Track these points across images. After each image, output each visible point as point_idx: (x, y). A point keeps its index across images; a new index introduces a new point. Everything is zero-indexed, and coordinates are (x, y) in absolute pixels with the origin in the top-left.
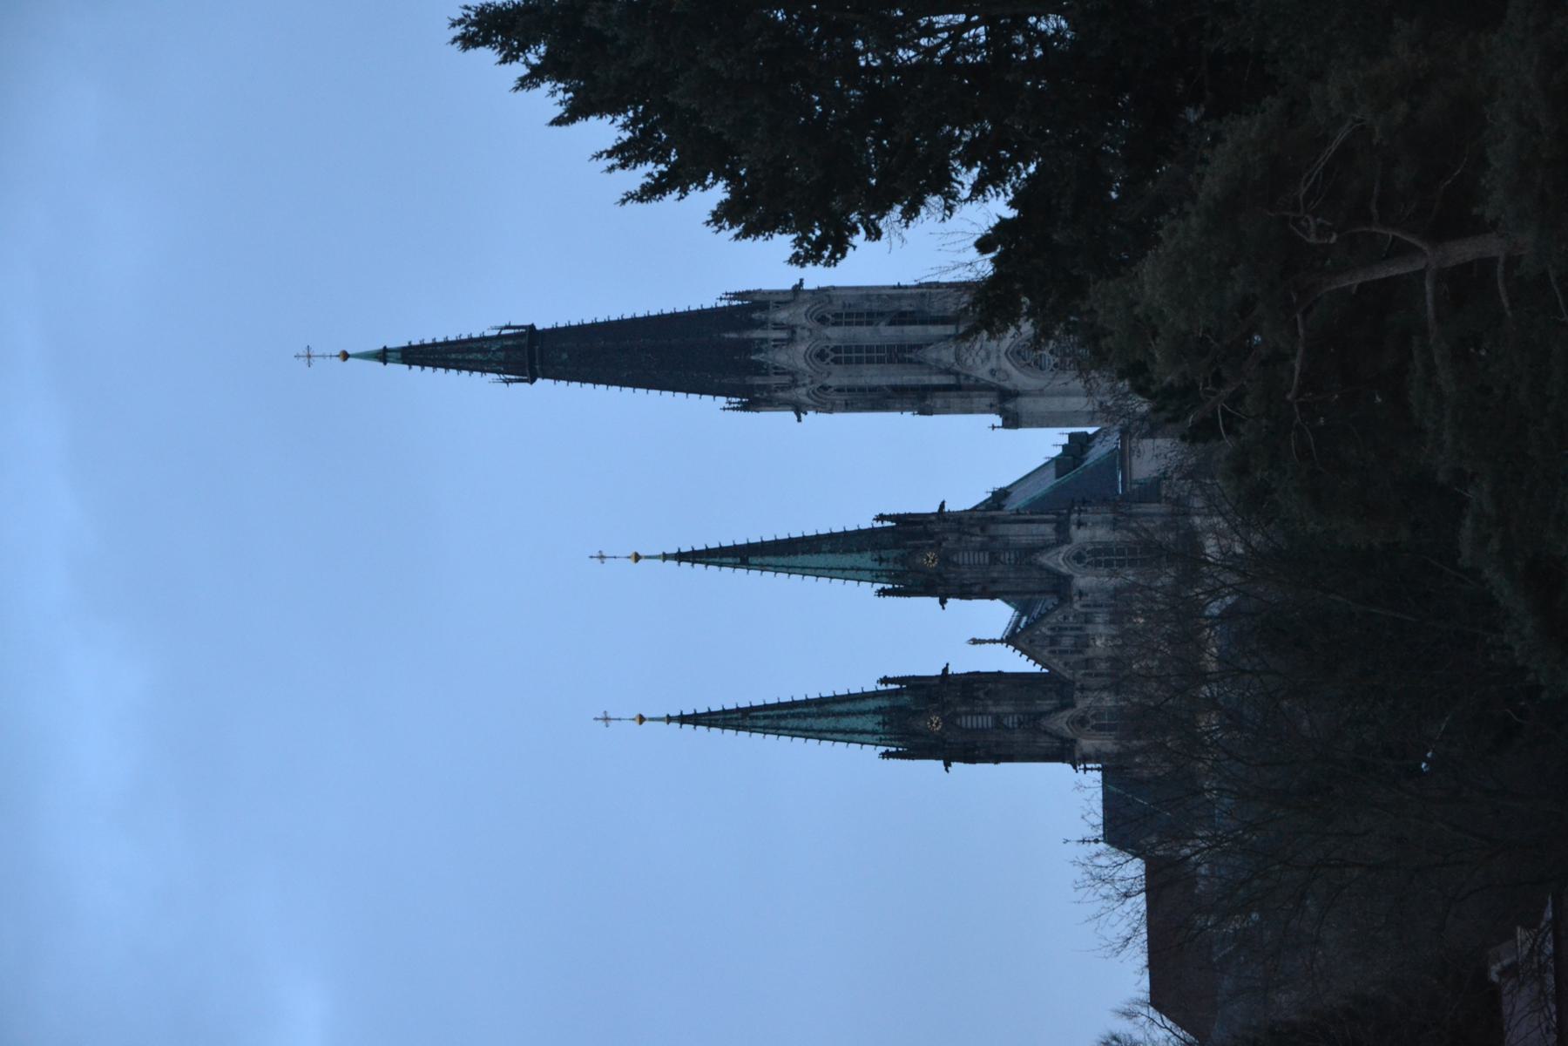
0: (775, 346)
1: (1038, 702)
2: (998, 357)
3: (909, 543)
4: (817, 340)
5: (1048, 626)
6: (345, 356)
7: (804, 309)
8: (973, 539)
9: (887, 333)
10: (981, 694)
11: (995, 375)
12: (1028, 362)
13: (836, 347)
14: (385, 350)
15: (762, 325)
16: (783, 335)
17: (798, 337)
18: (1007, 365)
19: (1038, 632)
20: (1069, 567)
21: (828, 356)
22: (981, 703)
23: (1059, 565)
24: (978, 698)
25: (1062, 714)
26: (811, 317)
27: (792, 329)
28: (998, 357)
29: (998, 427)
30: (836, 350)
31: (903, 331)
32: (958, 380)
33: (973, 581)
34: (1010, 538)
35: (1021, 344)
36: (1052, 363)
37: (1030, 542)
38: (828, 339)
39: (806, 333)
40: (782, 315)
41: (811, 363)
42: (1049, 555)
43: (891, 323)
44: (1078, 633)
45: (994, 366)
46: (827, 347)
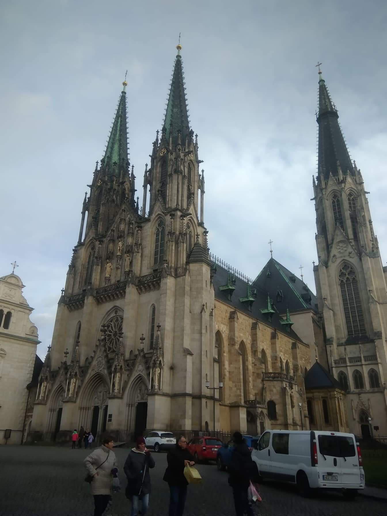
0: (336, 179)
2: (341, 257)
3: (171, 139)
8: (171, 167)
9: (347, 214)
11: (334, 257)
12: (342, 270)
13: (339, 200)
15: (345, 173)
18: (339, 261)
19: (128, 213)
20: (154, 219)
21: (335, 199)
23: (155, 213)
24: (106, 196)
26: (350, 190)
27: (344, 181)
28: (341, 257)
29: (314, 265)
30: (338, 201)
31: (347, 219)
32: (330, 245)
35: (349, 266)
36: (342, 279)
37: (168, 195)
38: (341, 195)
41: (331, 193)
43: (350, 215)
44: (126, 232)
45: (337, 256)
46: (339, 197)
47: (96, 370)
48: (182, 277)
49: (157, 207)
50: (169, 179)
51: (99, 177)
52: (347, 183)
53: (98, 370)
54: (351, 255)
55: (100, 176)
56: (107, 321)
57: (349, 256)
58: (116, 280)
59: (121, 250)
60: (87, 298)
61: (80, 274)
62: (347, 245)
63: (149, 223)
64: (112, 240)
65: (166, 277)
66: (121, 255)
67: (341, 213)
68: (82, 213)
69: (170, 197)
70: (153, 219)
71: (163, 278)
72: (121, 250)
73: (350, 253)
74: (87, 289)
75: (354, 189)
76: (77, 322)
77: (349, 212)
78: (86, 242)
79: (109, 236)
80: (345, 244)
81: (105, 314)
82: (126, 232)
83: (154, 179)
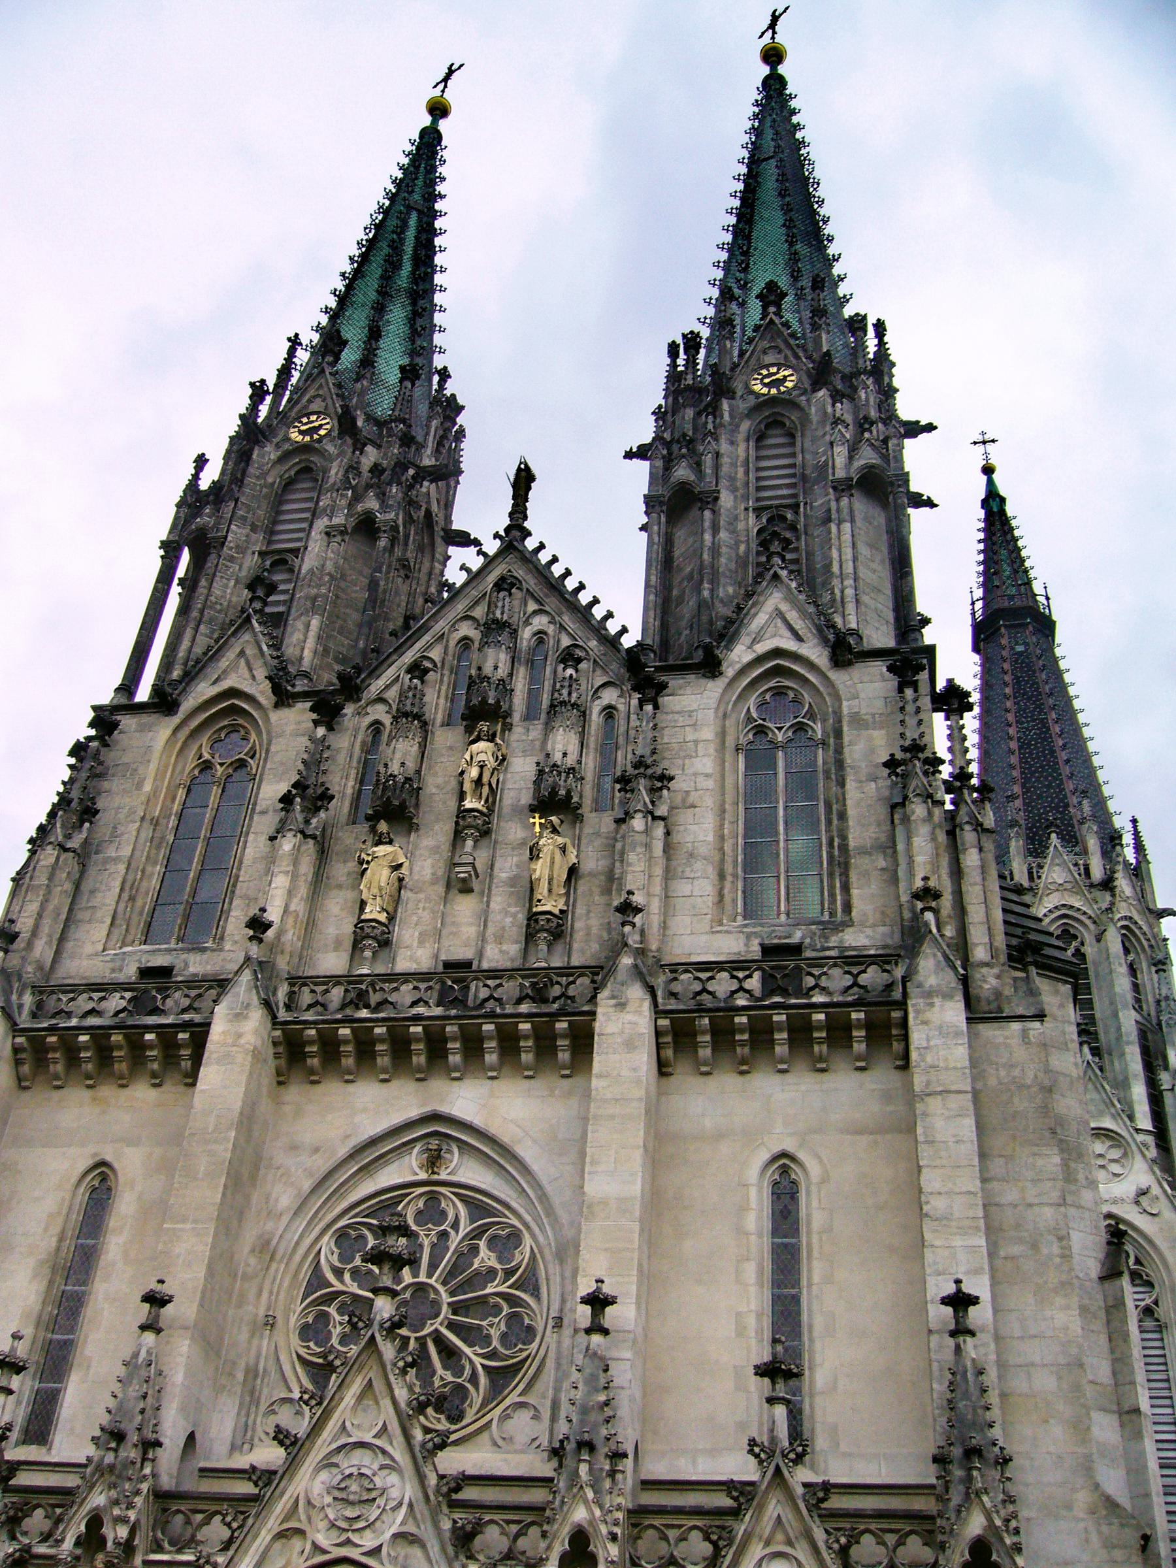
0: (1076, 865)
1: (315, 622)
4: (1095, 922)
5: (551, 629)
6: (988, 470)
7: (1137, 917)
10: (371, 503)
13: (1084, 955)
14: (1003, 500)
16: (1097, 873)
17: (1098, 894)
20: (743, 671)
22: (344, 502)
23: (755, 641)
25: (261, 673)
27: (1107, 884)
31: (1128, 1043)
33: (708, 460)
34: (847, 527)
37: (835, 568)
38: (1099, 938)
39: (1104, 906)
40: (1123, 884)
42: (793, 616)
46: (1082, 944)
47: (322, 1540)
48: (1016, 1026)
49: (761, 619)
50: (837, 500)
51: (306, 407)
52: (1118, 899)
53: (348, 1542)
54: (1144, 1200)
55: (310, 401)
56: (344, 1204)
57: (1137, 1203)
58: (443, 957)
59: (485, 790)
60: (239, 1016)
61: (122, 868)
62: (1125, 1155)
63: (711, 684)
64: (418, 717)
65: (947, 996)
66: (485, 810)
67: (1092, 1009)
68: (164, 545)
69: (849, 582)
70: (738, 667)
71: (929, 994)
72: (490, 784)
73: (1143, 1193)
74: (179, 966)
75: (1141, 928)
76: (83, 1164)
77: (1134, 1015)
78: (188, 704)
79: (380, 700)
80: (1111, 1147)
81: (343, 1151)
82: (519, 701)
83: (724, 483)
